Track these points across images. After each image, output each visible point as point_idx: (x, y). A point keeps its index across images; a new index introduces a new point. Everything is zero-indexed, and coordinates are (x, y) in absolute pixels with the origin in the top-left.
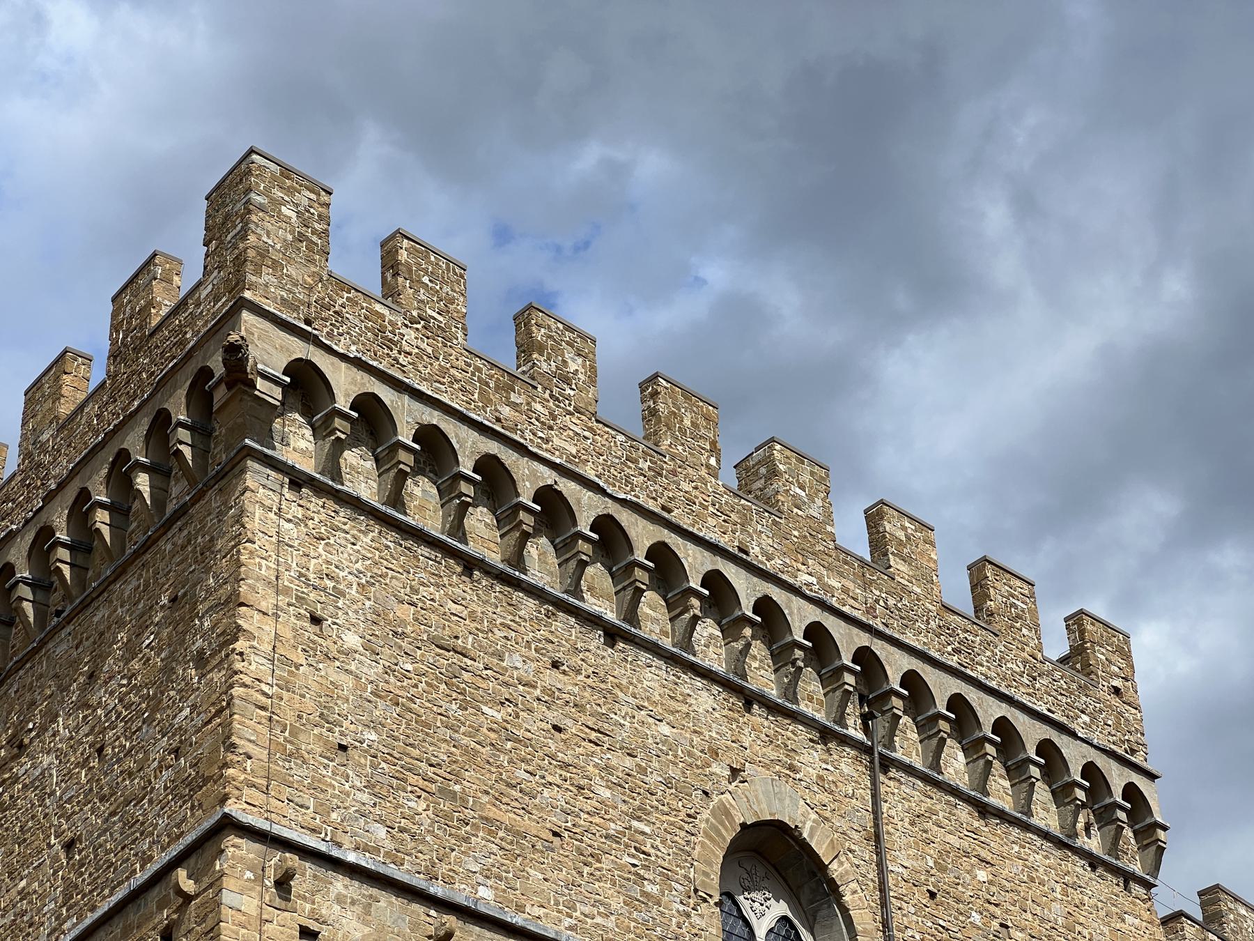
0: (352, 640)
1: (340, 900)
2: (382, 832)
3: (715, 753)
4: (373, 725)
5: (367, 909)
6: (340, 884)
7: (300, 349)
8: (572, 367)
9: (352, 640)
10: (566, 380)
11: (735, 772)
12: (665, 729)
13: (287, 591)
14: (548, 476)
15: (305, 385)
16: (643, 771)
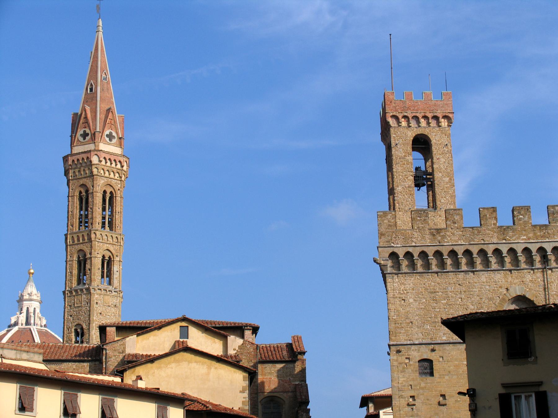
0: (411, 300)
1: (413, 350)
2: (420, 335)
3: (501, 287)
4: (417, 315)
5: (419, 350)
6: (413, 347)
7: (391, 250)
8: (456, 218)
9: (411, 300)
10: (455, 223)
11: (507, 289)
12: (488, 287)
13: (397, 297)
14: (450, 248)
15: (394, 256)
16: (481, 299)
